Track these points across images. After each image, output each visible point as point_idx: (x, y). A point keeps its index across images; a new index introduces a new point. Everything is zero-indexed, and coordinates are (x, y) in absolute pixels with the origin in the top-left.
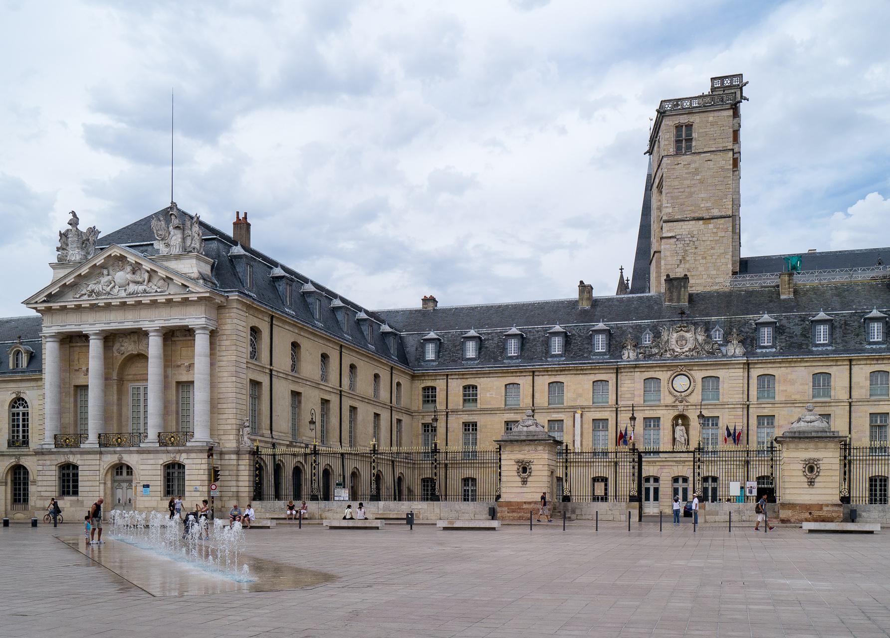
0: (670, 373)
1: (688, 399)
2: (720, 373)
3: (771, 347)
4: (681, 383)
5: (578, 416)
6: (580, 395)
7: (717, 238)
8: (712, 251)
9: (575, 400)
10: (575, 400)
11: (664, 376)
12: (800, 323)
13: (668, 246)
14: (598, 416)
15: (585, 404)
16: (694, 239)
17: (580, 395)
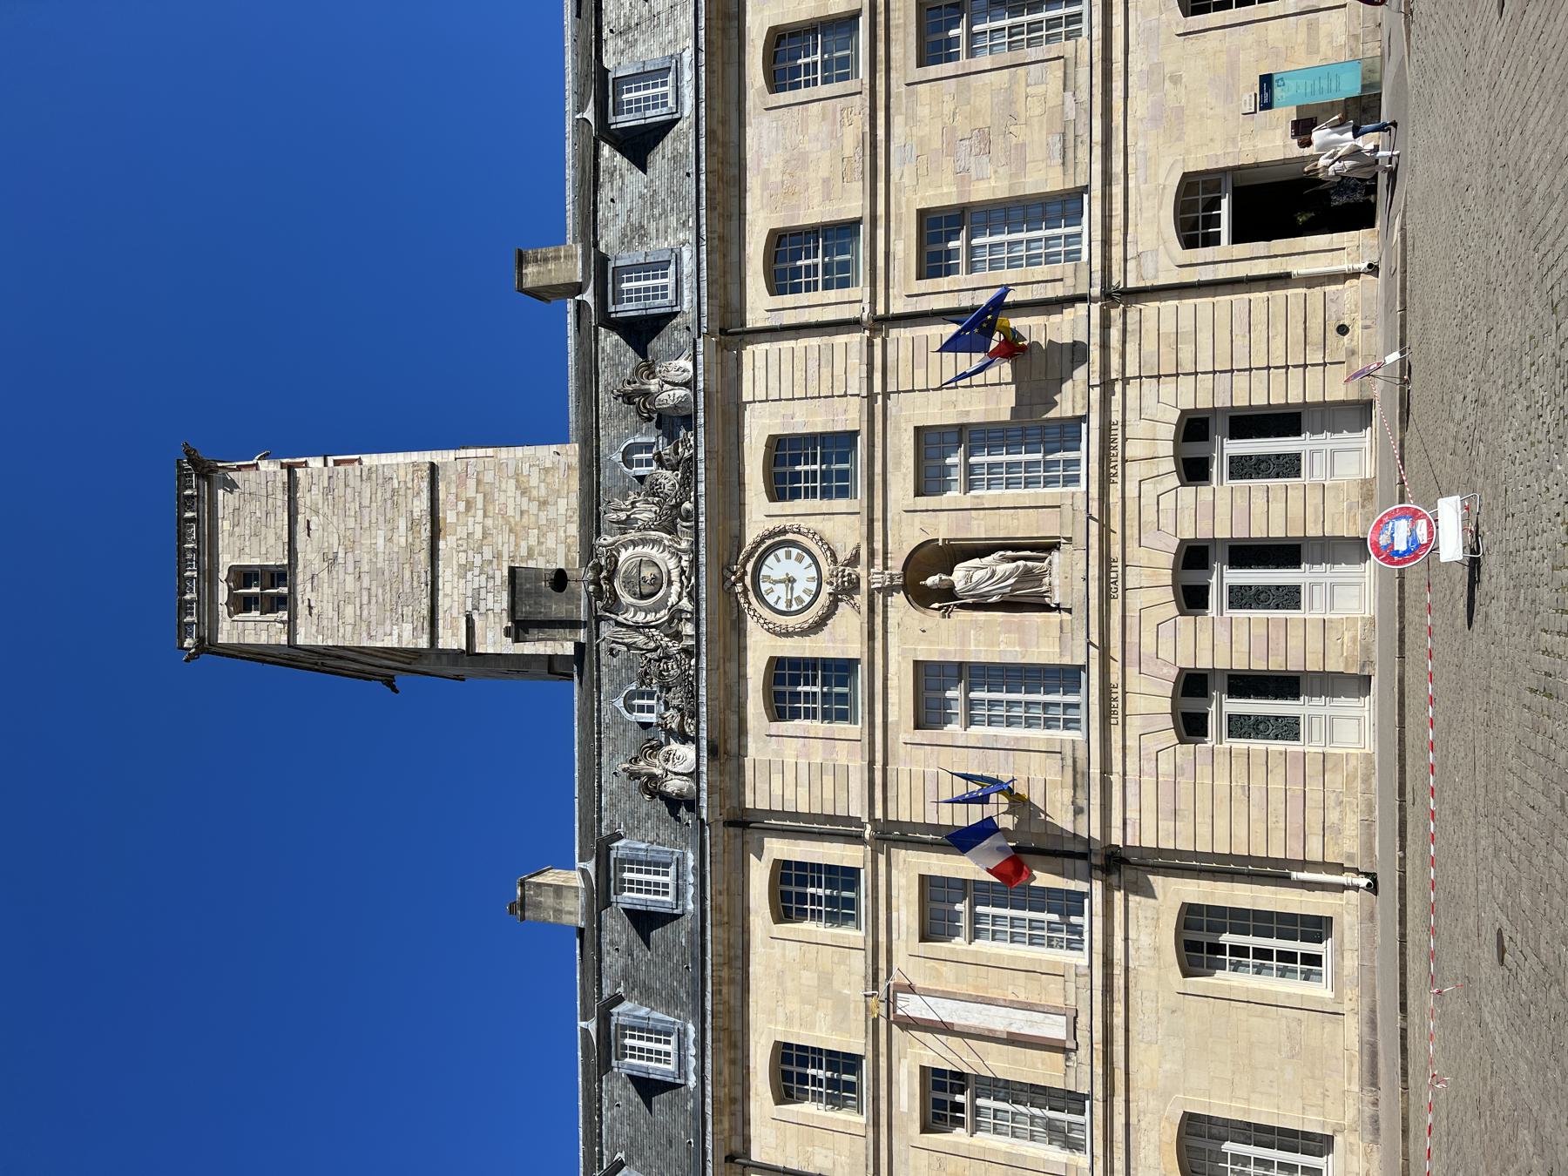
0: (751, 624)
1: (842, 557)
2: (758, 428)
3: (679, 258)
4: (789, 578)
5: (911, 1006)
6: (825, 980)
7: (480, 497)
8: (510, 512)
9: (841, 1003)
10: (841, 1003)
11: (761, 648)
12: (618, 182)
13: (490, 635)
14: (906, 914)
15: (858, 963)
16: (478, 562)
17: (825, 980)
